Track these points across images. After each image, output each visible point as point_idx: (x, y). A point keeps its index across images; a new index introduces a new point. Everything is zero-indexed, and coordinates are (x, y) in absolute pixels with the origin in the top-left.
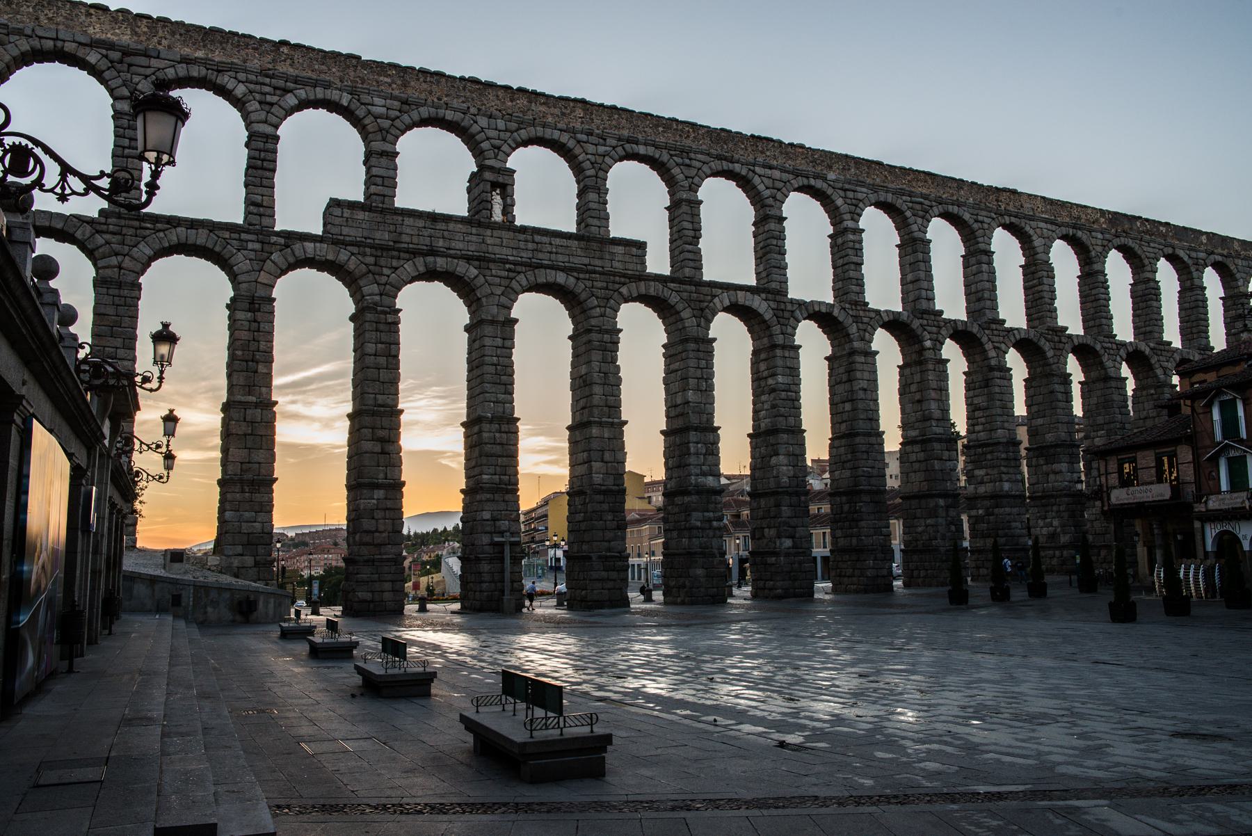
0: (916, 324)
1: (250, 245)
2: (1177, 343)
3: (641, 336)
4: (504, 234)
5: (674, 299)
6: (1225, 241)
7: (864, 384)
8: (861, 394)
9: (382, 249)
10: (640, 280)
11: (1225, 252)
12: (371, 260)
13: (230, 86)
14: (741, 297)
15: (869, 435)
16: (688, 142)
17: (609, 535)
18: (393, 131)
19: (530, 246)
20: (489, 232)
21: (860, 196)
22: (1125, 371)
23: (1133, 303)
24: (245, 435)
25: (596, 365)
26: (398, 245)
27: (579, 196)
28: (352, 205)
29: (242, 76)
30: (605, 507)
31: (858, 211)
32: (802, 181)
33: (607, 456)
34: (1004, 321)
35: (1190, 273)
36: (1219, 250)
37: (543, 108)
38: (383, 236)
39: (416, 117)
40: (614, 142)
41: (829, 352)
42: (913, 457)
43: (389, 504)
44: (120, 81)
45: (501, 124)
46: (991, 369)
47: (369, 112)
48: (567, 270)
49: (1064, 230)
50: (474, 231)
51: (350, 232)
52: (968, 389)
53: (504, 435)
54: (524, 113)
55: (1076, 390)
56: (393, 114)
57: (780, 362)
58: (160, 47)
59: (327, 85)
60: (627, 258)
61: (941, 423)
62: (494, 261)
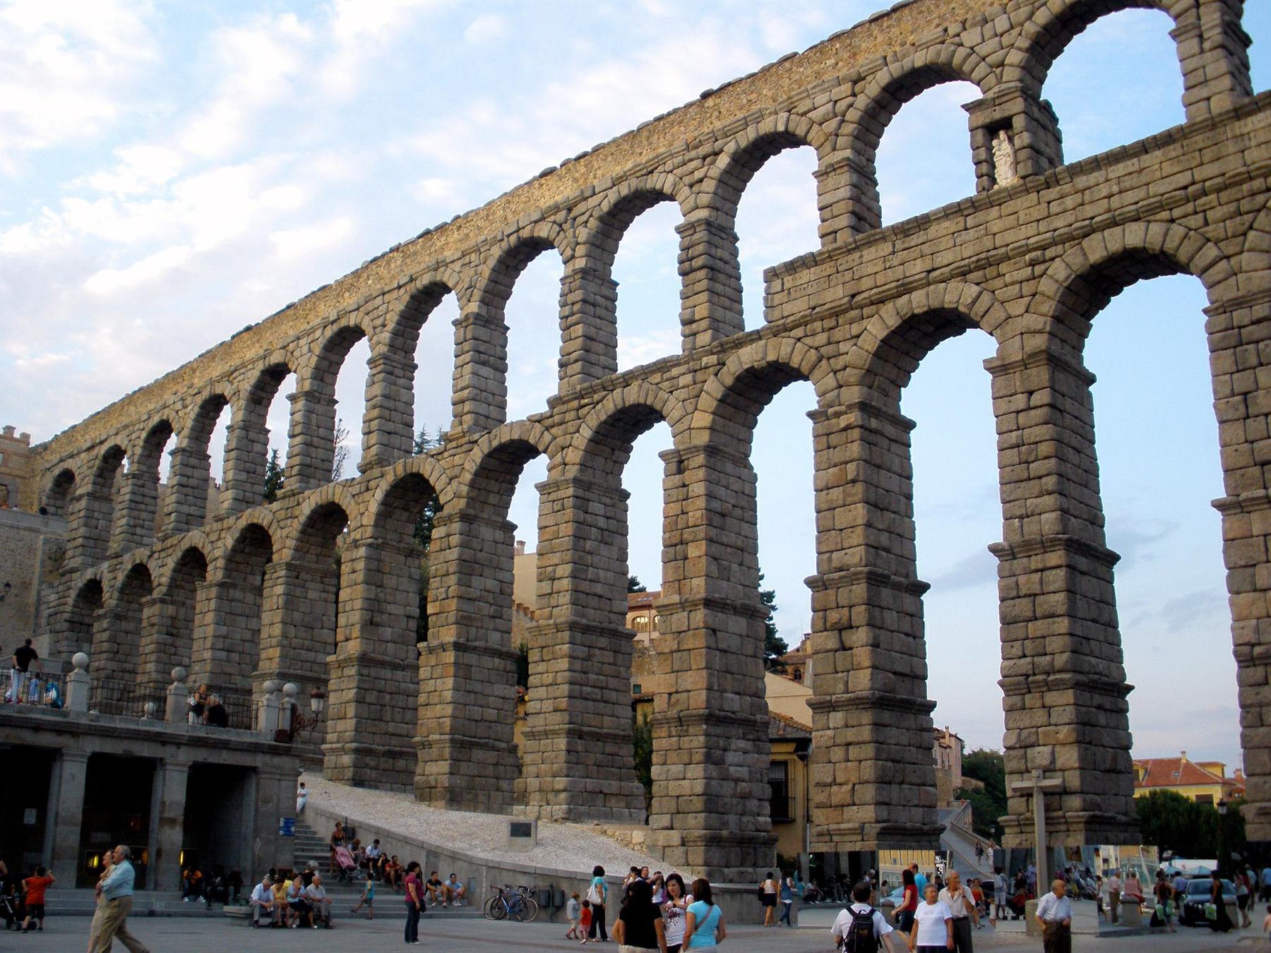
1: (683, 381)
4: (1020, 203)
9: (837, 315)
13: (658, 187)
19: (1069, 202)
20: (994, 212)
24: (672, 652)
26: (858, 298)
28: (791, 267)
38: (836, 294)
43: (851, 735)
44: (564, 244)
50: (970, 221)
51: (798, 307)
53: (1036, 577)
56: (841, 106)
58: (596, 182)
59: (760, 117)
62: (1007, 258)
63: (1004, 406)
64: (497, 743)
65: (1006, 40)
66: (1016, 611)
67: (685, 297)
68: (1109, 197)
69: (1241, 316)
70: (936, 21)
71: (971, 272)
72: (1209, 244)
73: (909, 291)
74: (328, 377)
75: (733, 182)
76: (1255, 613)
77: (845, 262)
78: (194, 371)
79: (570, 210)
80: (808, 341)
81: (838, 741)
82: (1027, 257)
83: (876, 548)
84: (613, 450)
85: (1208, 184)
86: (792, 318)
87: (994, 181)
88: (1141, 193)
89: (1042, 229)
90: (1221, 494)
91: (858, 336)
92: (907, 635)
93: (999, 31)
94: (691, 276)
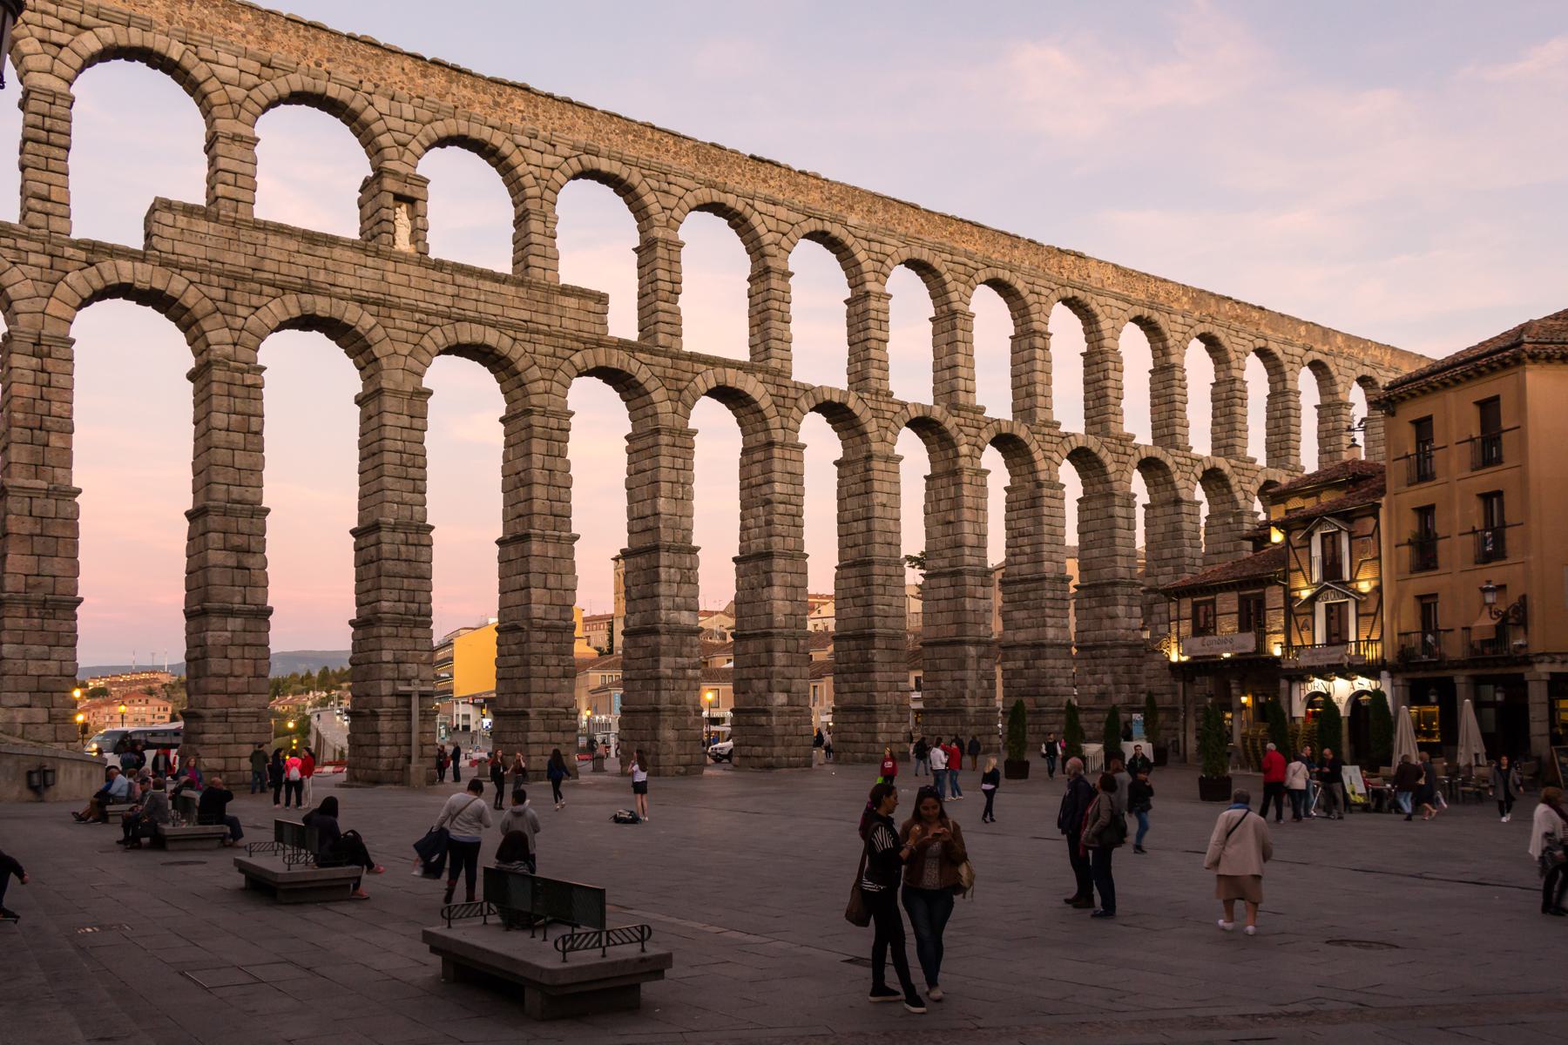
0: (950, 423)
2: (1262, 461)
3: (597, 425)
4: (413, 270)
5: (642, 375)
6: (1327, 333)
7: (882, 498)
8: (878, 511)
10: (599, 345)
11: (1326, 349)
14: (733, 379)
15: (888, 564)
16: (667, 159)
18: (249, 105)
19: (450, 289)
20: (391, 266)
21: (889, 250)
22: (1199, 494)
23: (1214, 408)
25: (537, 460)
27: (517, 223)
28: (189, 210)
31: (885, 269)
32: (814, 225)
34: (1059, 424)
35: (1283, 373)
36: (1318, 346)
37: (468, 93)
38: (237, 259)
40: (567, 152)
41: (838, 453)
42: (942, 593)
46: (1039, 485)
49: (1137, 311)
50: (370, 262)
51: (189, 251)
52: (1009, 509)
54: (441, 96)
55: (1140, 514)
56: (250, 80)
57: (777, 465)
60: (582, 315)
61: (976, 552)
62: (398, 307)
65: (409, 125)
69: (553, 422)
70: (352, 68)
77: (245, 234)
82: (417, 316)
88: (498, 311)
89: (428, 298)
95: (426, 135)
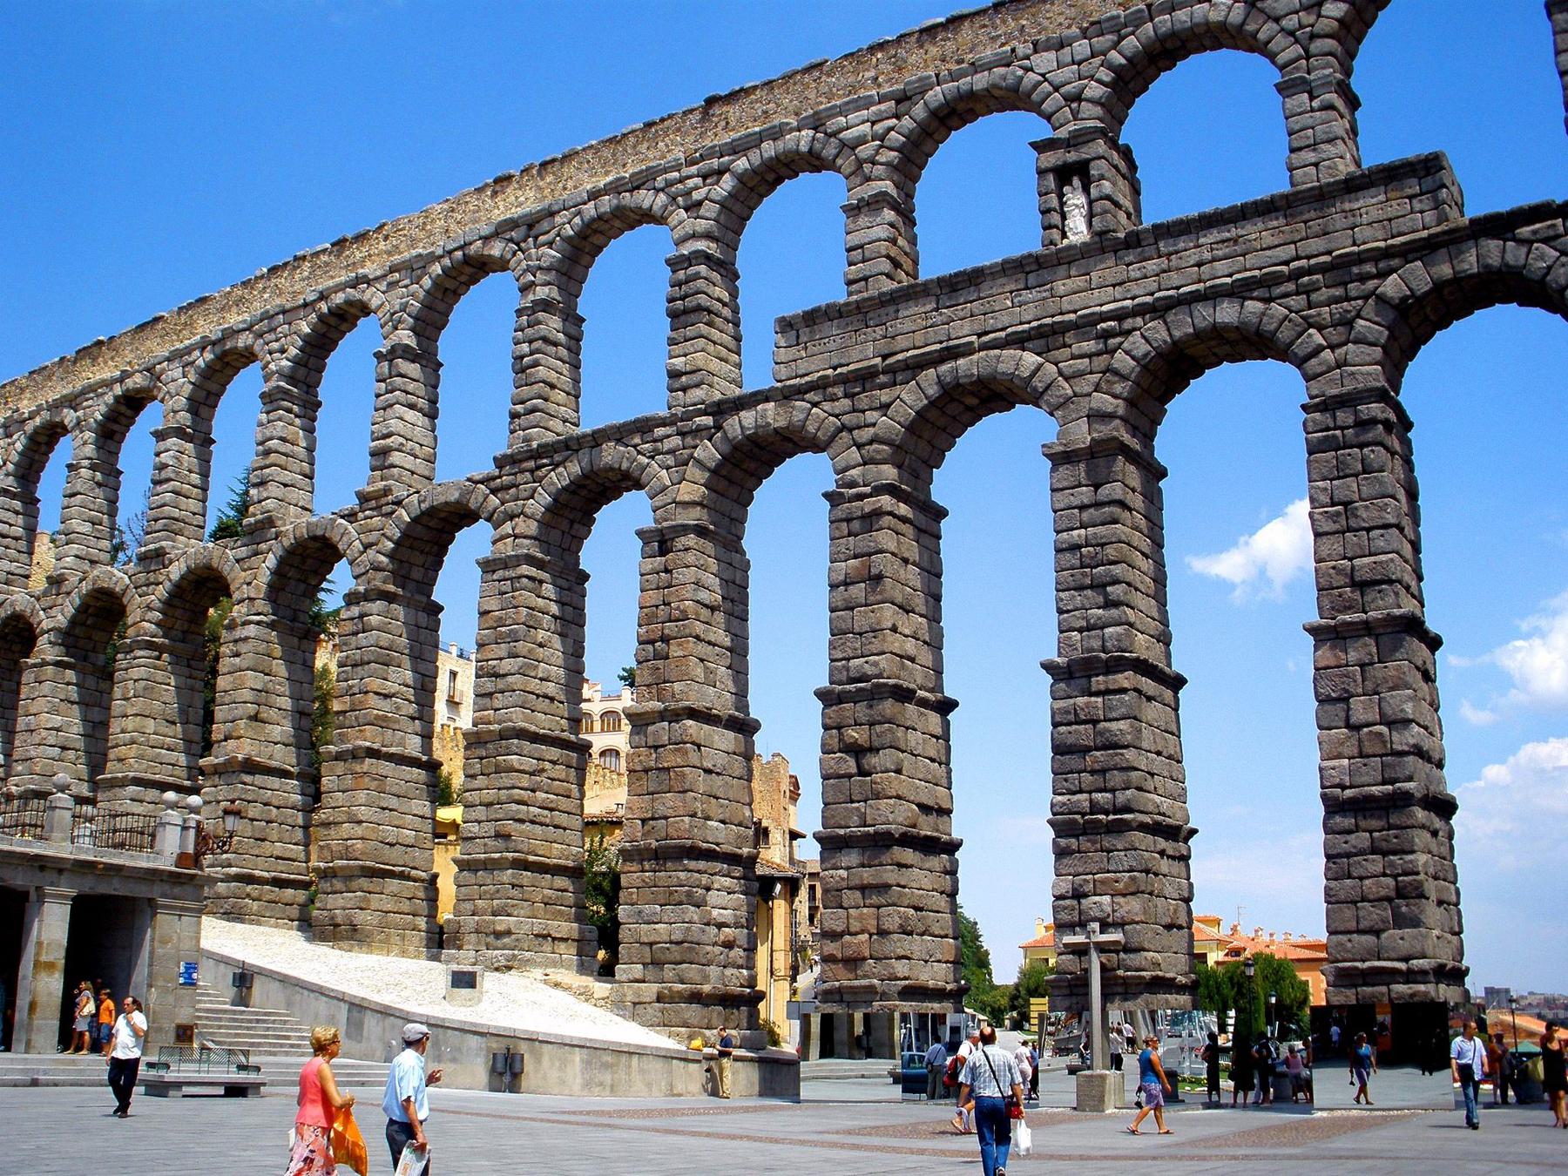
1: (668, 444)
12: (845, 403)
17: (1373, 914)
19: (1152, 265)
24: (646, 771)
28: (813, 318)
29: (660, 182)
30: (1361, 839)
33: (1361, 709)
38: (864, 352)
39: (919, 111)
43: (867, 876)
45: (1081, 48)
47: (843, 144)
48: (1240, 291)
50: (1032, 279)
51: (816, 366)
59: (776, 133)
63: (1064, 499)
64: (414, 872)
66: (1070, 740)
67: (672, 342)
68: (1199, 265)
71: (1030, 339)
72: (1311, 331)
73: (956, 357)
74: (204, 411)
75: (737, 207)
76: (1347, 751)
78: (22, 390)
79: (530, 227)
80: (827, 406)
81: (852, 884)
83: (901, 657)
84: (572, 522)
85: (1313, 261)
86: (807, 379)
87: (1064, 235)
89: (1118, 296)
90: (1315, 618)
91: (888, 406)
92: (933, 760)
93: (1077, 58)
94: (682, 318)
95: (1111, 67)
